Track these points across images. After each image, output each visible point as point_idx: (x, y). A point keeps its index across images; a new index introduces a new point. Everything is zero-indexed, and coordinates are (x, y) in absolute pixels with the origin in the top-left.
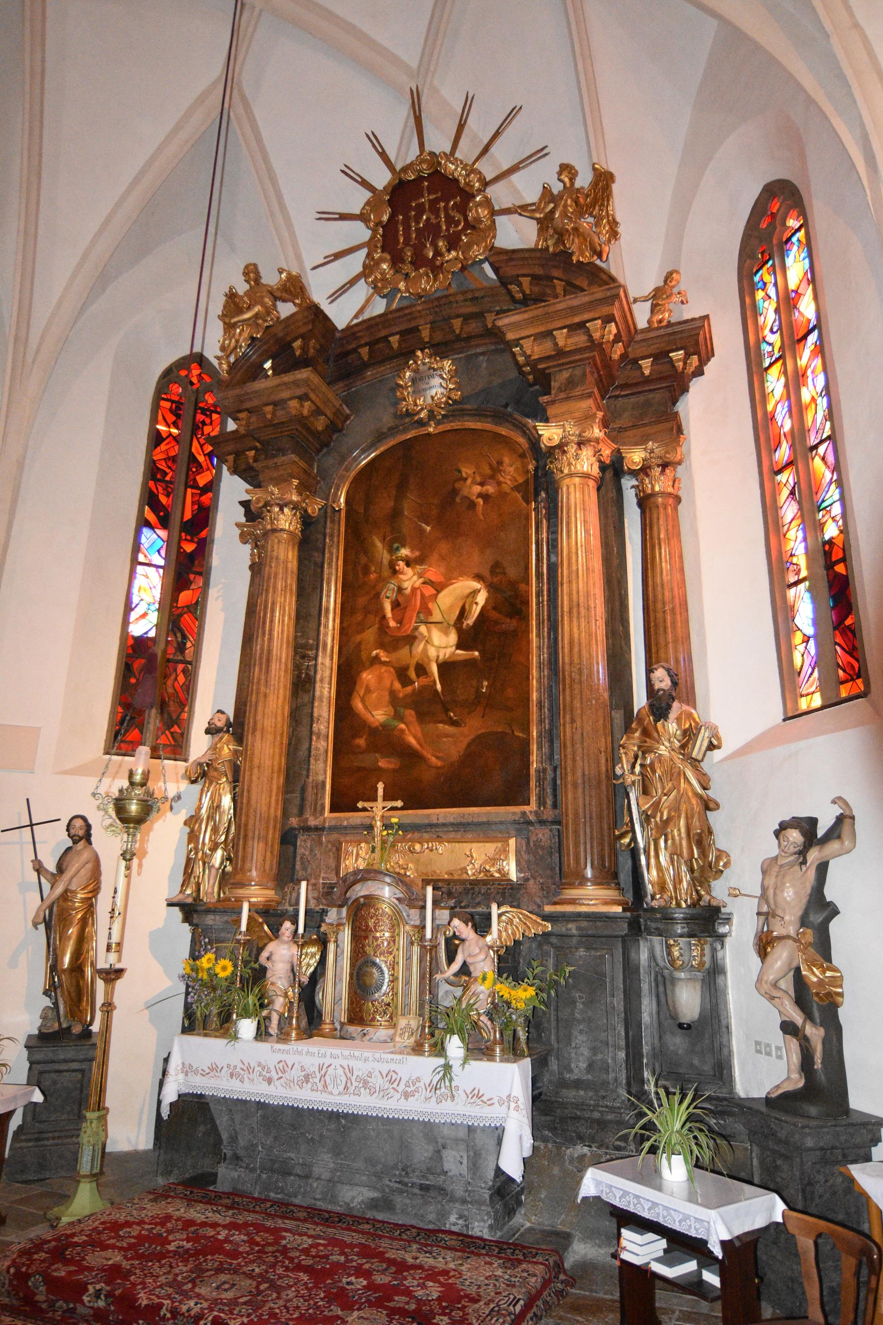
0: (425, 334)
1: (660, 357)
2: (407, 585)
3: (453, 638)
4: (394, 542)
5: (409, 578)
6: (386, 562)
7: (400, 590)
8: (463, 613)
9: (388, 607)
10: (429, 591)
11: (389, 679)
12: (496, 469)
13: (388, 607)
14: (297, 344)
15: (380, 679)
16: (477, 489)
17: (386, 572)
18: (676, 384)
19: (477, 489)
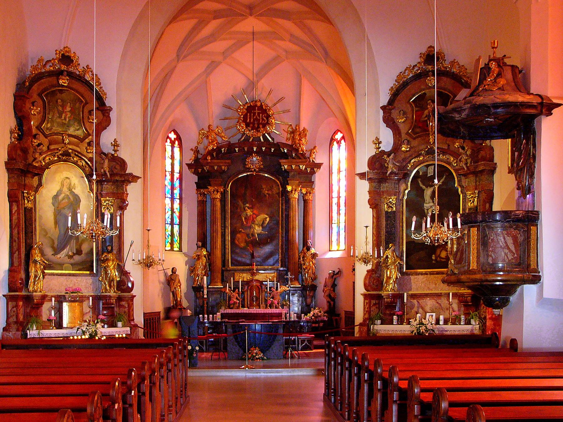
0: (255, 149)
1: (312, 169)
2: (249, 214)
3: (261, 228)
4: (244, 203)
5: (249, 212)
6: (242, 207)
7: (247, 215)
8: (263, 223)
9: (243, 219)
10: (254, 216)
11: (245, 237)
12: (271, 189)
13: (243, 219)
14: (223, 150)
15: (242, 236)
16: (267, 192)
17: (243, 210)
18: (313, 173)
19: (267, 192)
